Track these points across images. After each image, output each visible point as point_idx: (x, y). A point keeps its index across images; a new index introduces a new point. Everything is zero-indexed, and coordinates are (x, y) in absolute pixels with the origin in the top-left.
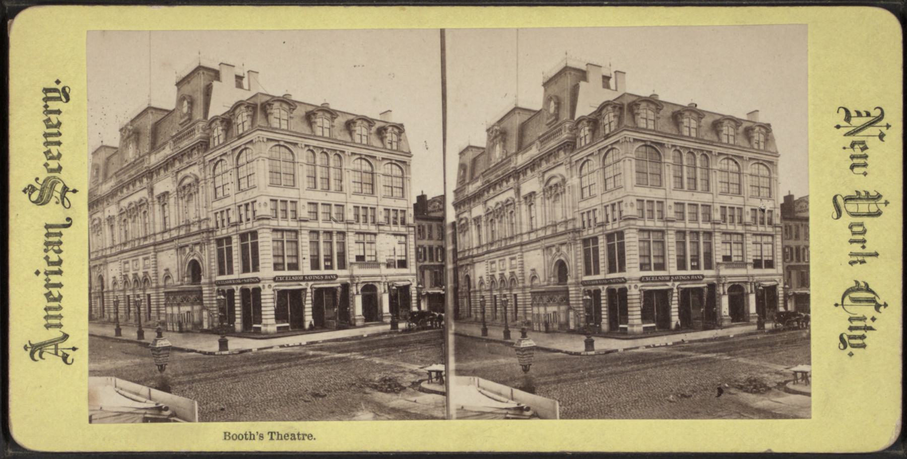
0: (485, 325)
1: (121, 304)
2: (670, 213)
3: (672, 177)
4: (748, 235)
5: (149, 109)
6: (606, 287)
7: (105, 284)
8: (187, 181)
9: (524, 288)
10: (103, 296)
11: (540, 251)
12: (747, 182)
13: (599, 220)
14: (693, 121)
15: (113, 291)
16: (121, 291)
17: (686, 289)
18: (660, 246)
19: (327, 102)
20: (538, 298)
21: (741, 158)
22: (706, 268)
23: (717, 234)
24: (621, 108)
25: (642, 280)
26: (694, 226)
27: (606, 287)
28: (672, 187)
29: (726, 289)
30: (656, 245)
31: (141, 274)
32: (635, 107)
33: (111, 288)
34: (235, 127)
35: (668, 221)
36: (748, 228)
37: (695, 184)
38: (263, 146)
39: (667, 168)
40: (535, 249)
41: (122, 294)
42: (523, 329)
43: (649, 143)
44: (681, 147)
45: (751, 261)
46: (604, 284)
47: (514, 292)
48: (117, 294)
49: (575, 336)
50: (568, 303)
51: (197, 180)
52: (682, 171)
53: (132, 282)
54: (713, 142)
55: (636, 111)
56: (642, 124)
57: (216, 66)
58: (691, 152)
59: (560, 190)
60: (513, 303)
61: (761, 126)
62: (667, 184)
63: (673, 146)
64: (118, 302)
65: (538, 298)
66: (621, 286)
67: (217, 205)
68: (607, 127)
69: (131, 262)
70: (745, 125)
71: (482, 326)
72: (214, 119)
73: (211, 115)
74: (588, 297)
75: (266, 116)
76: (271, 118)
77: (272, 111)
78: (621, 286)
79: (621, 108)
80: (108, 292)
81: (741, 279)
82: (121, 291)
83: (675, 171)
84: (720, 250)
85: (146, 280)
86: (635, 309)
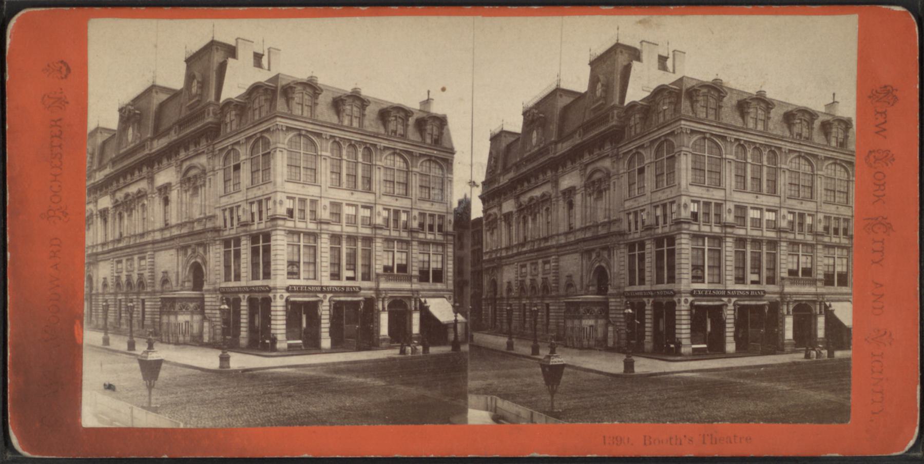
0: (131, 336)
1: (111, 309)
2: (325, 215)
3: (328, 172)
4: (820, 247)
5: (152, 89)
6: (247, 296)
7: (95, 285)
8: (193, 173)
9: (154, 292)
10: (91, 299)
11: (173, 252)
12: (820, 185)
13: (243, 219)
14: (355, 109)
15: (103, 294)
16: (111, 294)
17: (744, 305)
18: (312, 251)
19: (359, 86)
20: (168, 305)
21: (815, 156)
22: (363, 279)
23: (378, 240)
24: (274, 92)
25: (692, 293)
26: (756, 233)
27: (247, 296)
28: (733, 187)
29: (791, 309)
30: (307, 250)
31: (135, 277)
32: (289, 91)
33: (100, 291)
34: (250, 113)
35: (321, 223)
36: (819, 238)
37: (760, 185)
38: (281, 135)
39: (323, 162)
40: (166, 249)
41: (112, 297)
42: (149, 340)
43: (304, 133)
44: (745, 141)
45: (821, 277)
46: (245, 292)
47: (142, 297)
48: (107, 297)
49: (208, 350)
50: (202, 312)
51: (204, 172)
52: (340, 167)
53: (125, 286)
54: (378, 134)
55: (290, 96)
56: (297, 111)
57: (232, 42)
58: (353, 145)
59: (199, 183)
60: (140, 309)
61: (841, 121)
62: (323, 179)
63: (332, 137)
64: (108, 306)
65: (168, 305)
66: (264, 295)
67: (224, 201)
68: (257, 112)
69: (124, 261)
70: (822, 118)
71: (127, 339)
72: (228, 103)
73: (224, 96)
74: (226, 307)
75: (288, 101)
76: (293, 103)
77: (294, 96)
78: (264, 295)
79: (274, 92)
80: (97, 294)
81: (810, 298)
82: (111, 294)
83: (332, 165)
84: (786, 262)
85: (141, 283)
86: (279, 322)
